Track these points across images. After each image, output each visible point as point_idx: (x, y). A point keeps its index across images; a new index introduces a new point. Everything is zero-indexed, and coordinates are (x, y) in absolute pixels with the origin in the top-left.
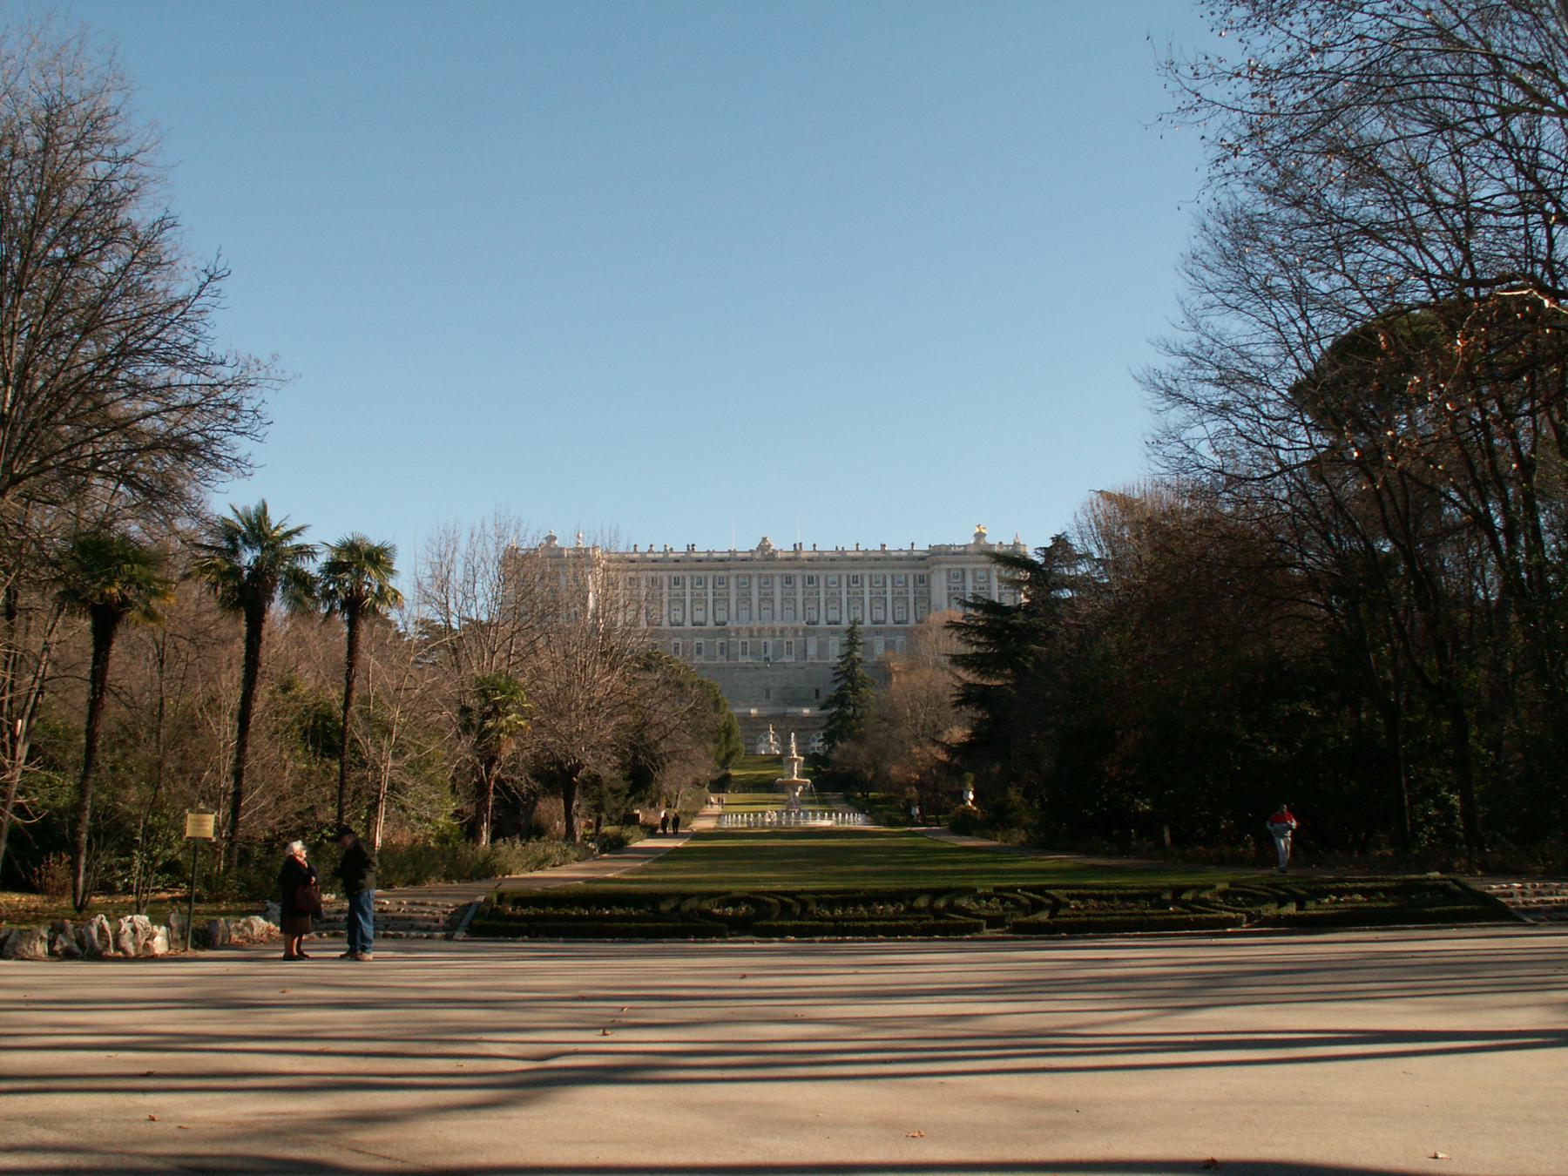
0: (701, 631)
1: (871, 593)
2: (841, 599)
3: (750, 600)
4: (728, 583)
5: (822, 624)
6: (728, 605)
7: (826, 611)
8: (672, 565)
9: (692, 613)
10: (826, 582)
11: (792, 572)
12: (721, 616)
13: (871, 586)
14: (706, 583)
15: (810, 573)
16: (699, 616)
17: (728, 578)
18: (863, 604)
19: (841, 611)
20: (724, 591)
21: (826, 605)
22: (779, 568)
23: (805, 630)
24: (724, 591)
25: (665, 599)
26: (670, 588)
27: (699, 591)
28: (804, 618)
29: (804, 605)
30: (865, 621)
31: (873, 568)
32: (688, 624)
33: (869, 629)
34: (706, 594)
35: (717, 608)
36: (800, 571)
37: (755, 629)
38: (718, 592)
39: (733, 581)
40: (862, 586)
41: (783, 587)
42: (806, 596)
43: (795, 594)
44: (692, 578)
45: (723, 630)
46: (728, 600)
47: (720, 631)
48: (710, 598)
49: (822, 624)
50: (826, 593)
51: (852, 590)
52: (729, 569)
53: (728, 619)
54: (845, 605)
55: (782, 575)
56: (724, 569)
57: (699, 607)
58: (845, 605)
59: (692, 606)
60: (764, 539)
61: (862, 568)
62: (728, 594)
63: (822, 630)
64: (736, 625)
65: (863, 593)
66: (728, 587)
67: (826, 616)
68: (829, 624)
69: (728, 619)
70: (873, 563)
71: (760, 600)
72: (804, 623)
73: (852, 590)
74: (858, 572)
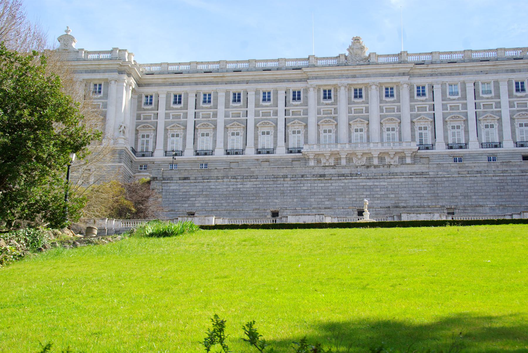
0: (267, 161)
1: (511, 105)
2: (466, 115)
3: (335, 119)
4: (306, 97)
5: (440, 148)
6: (306, 126)
7: (445, 131)
8: (230, 76)
9: (256, 138)
10: (444, 93)
11: (395, 80)
12: (294, 141)
13: (510, 95)
14: (276, 99)
15: (418, 81)
16: (266, 142)
17: (306, 90)
18: (500, 120)
19: (467, 132)
20: (301, 109)
21: (445, 122)
22: (375, 75)
23: (415, 157)
24: (301, 109)
25: (221, 120)
26: (227, 106)
27: (265, 110)
28: (413, 139)
29: (412, 122)
30: (504, 144)
31: (513, 71)
32: (250, 152)
33: (513, 154)
34: (276, 113)
35: (290, 131)
36: (406, 79)
37: (343, 156)
38: (291, 109)
39: (312, 96)
40: (498, 96)
41: (381, 101)
42: (416, 112)
43: (399, 110)
44: (257, 92)
45: (298, 160)
46: (306, 121)
47: (293, 160)
48: (281, 117)
49: (440, 148)
50: (444, 107)
51: (482, 102)
52: (306, 80)
53: (306, 143)
54: (472, 123)
55: (381, 85)
56: (300, 80)
57: (266, 130)
58: (472, 123)
59: (256, 128)
60: (356, 40)
61: (497, 72)
62: (306, 113)
63: (440, 156)
64: (316, 149)
65: (498, 105)
66: (306, 104)
67: (446, 138)
68: (451, 148)
69: (306, 143)
70: (513, 64)
71: (350, 119)
72: (414, 146)
73: (482, 102)
74: (491, 78)
